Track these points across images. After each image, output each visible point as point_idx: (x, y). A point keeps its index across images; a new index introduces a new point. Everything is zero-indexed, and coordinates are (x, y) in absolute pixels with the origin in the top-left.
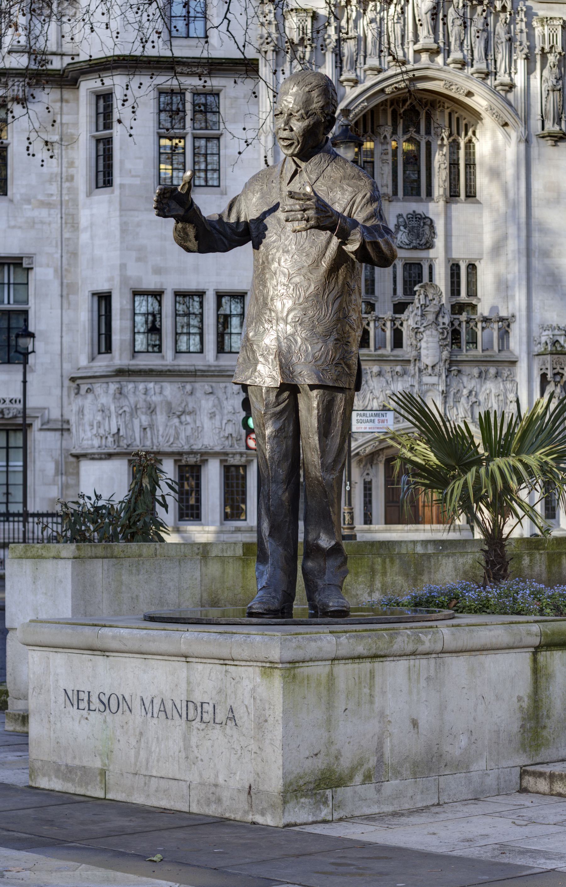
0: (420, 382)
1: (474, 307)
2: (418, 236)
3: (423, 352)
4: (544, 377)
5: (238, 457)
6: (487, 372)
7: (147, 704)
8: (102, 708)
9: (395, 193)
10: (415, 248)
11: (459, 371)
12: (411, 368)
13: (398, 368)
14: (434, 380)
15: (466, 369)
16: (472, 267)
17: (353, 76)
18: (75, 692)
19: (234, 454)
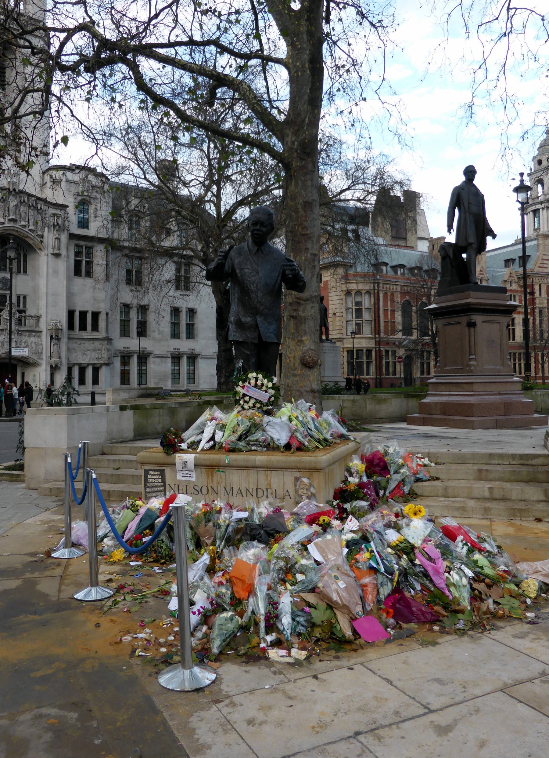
1: (25, 312)
4: (51, 337)
7: (228, 489)
8: (197, 493)
15: (24, 333)
16: (25, 298)
18: (177, 486)
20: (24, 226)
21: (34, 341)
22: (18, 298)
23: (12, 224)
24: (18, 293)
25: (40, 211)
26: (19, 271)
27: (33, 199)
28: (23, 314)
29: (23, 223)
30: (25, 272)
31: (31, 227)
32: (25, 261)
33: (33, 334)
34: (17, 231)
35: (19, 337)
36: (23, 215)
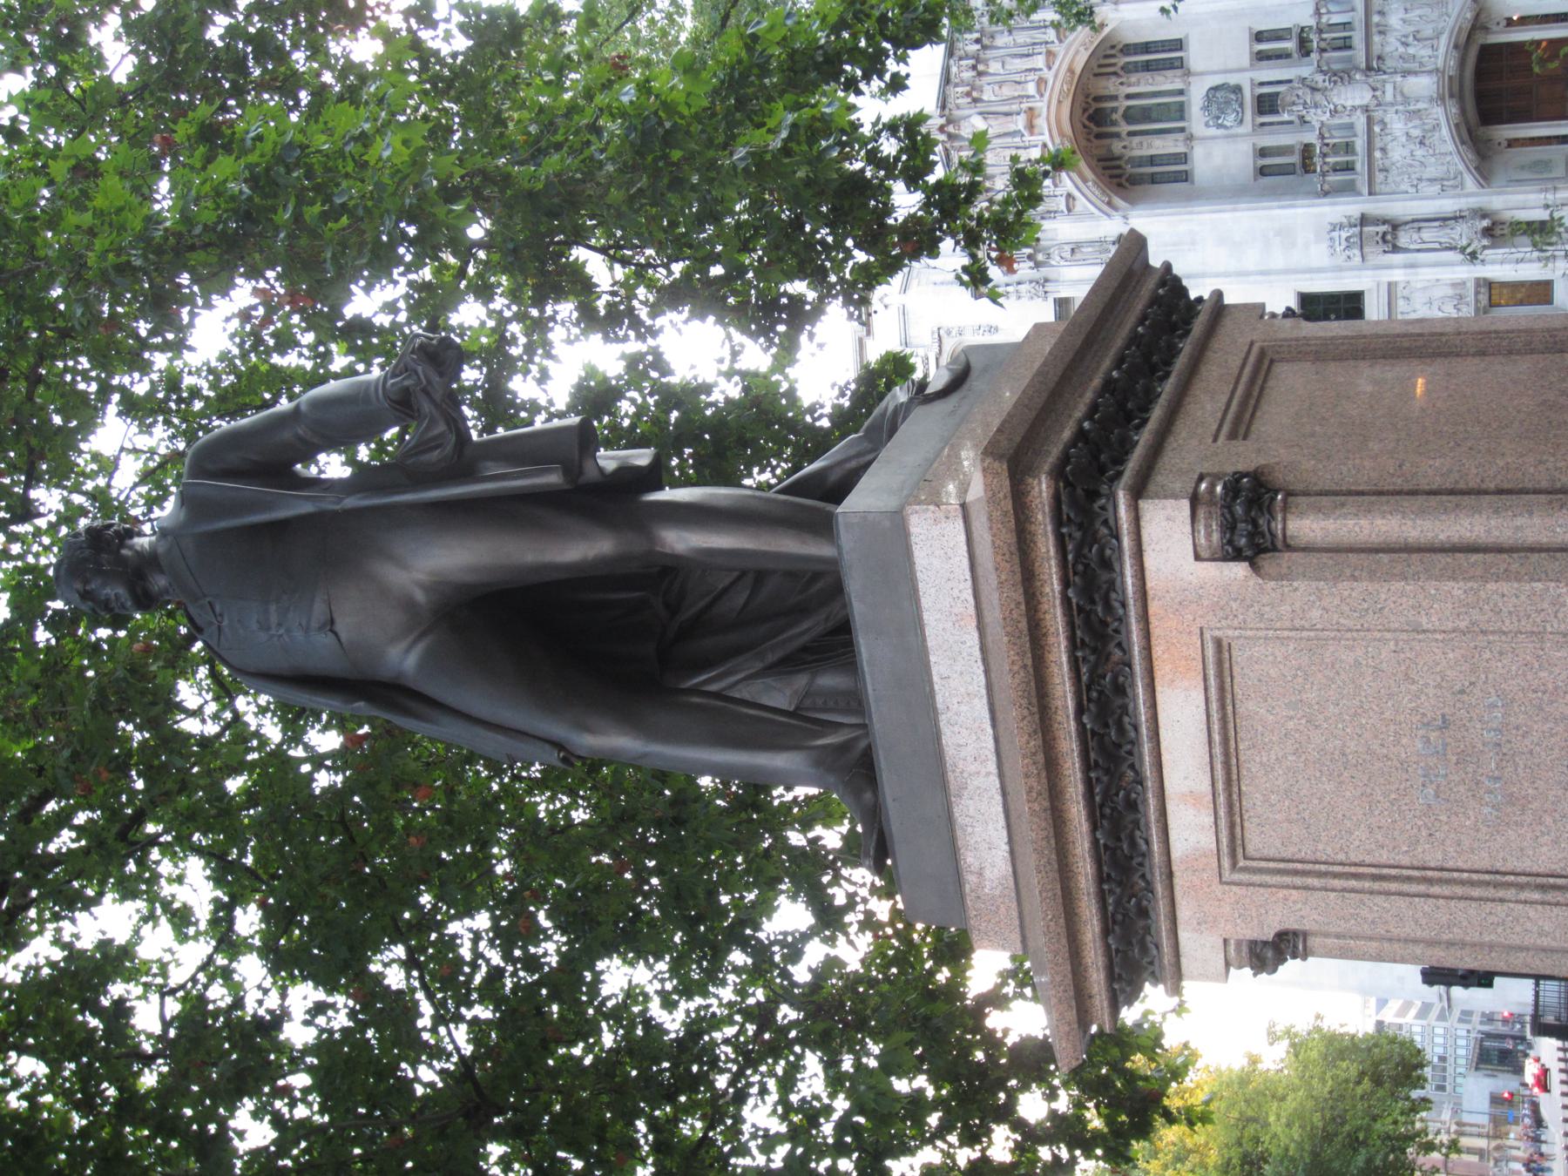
0: (1392, 105)
2: (1228, 102)
3: (1358, 102)
5: (1481, 297)
6: (1378, 25)
9: (1182, 130)
10: (1241, 105)
11: (1379, 58)
12: (1377, 115)
13: (1377, 129)
14: (1389, 88)
15: (1376, 49)
16: (1259, 37)
17: (1063, 200)
19: (1477, 301)
20: (1041, 82)
21: (1401, 15)
22: (1261, 57)
23: (1041, 123)
24: (1245, 60)
25: (986, 41)
26: (1178, 65)
27: (954, 69)
28: (1314, 37)
29: (1031, 89)
30: (1178, 45)
31: (1040, 62)
32: (1146, 47)
33: (1376, 19)
34: (1059, 102)
35: (1390, 63)
36: (1007, 91)
